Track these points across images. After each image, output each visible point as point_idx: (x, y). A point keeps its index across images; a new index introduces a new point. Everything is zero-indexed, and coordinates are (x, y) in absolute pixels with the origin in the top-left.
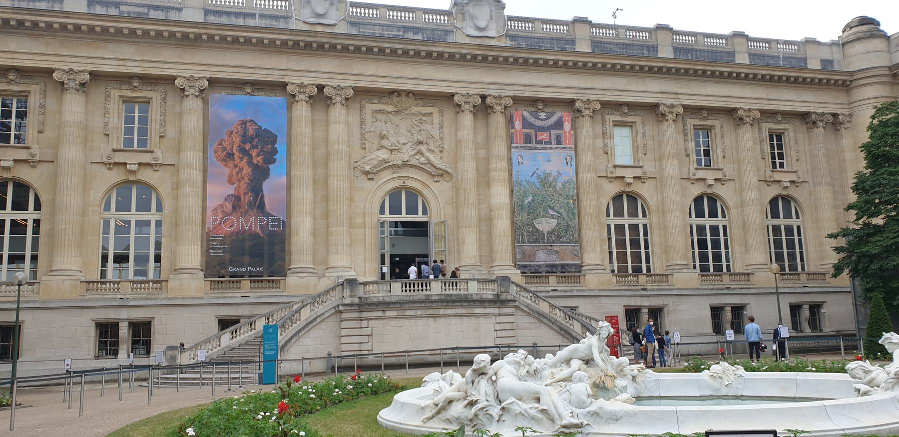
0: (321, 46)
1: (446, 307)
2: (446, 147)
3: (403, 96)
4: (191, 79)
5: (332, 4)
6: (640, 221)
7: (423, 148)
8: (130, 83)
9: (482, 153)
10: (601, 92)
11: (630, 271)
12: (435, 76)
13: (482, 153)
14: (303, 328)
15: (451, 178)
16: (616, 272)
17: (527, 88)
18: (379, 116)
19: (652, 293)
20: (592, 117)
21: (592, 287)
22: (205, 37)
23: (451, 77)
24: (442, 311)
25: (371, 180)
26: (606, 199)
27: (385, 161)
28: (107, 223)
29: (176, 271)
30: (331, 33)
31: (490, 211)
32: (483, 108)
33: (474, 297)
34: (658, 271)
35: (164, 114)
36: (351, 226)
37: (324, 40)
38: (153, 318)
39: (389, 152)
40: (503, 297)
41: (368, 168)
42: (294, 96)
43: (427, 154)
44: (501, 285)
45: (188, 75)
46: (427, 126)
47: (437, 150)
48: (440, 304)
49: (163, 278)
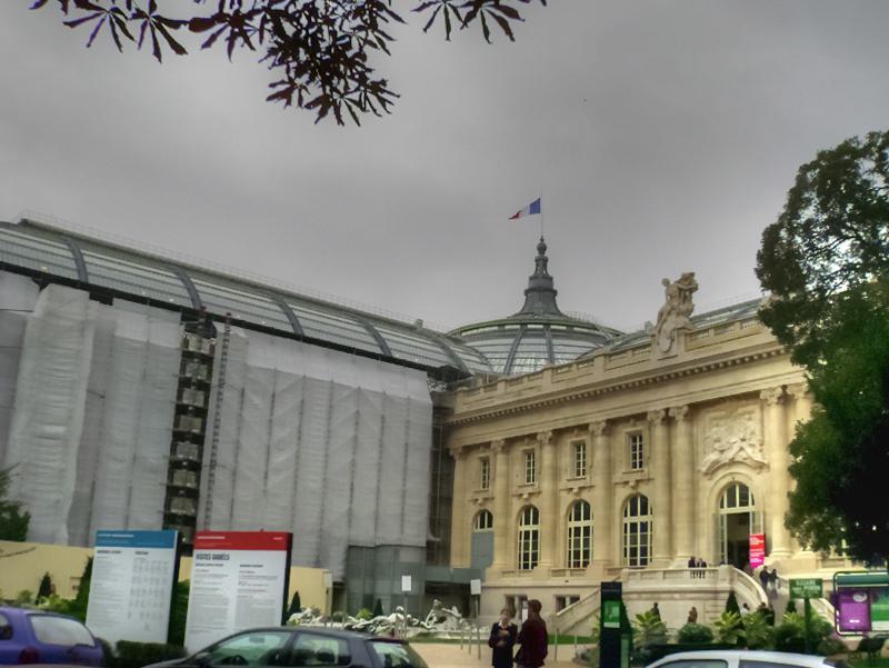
7: (744, 444)
27: (716, 462)
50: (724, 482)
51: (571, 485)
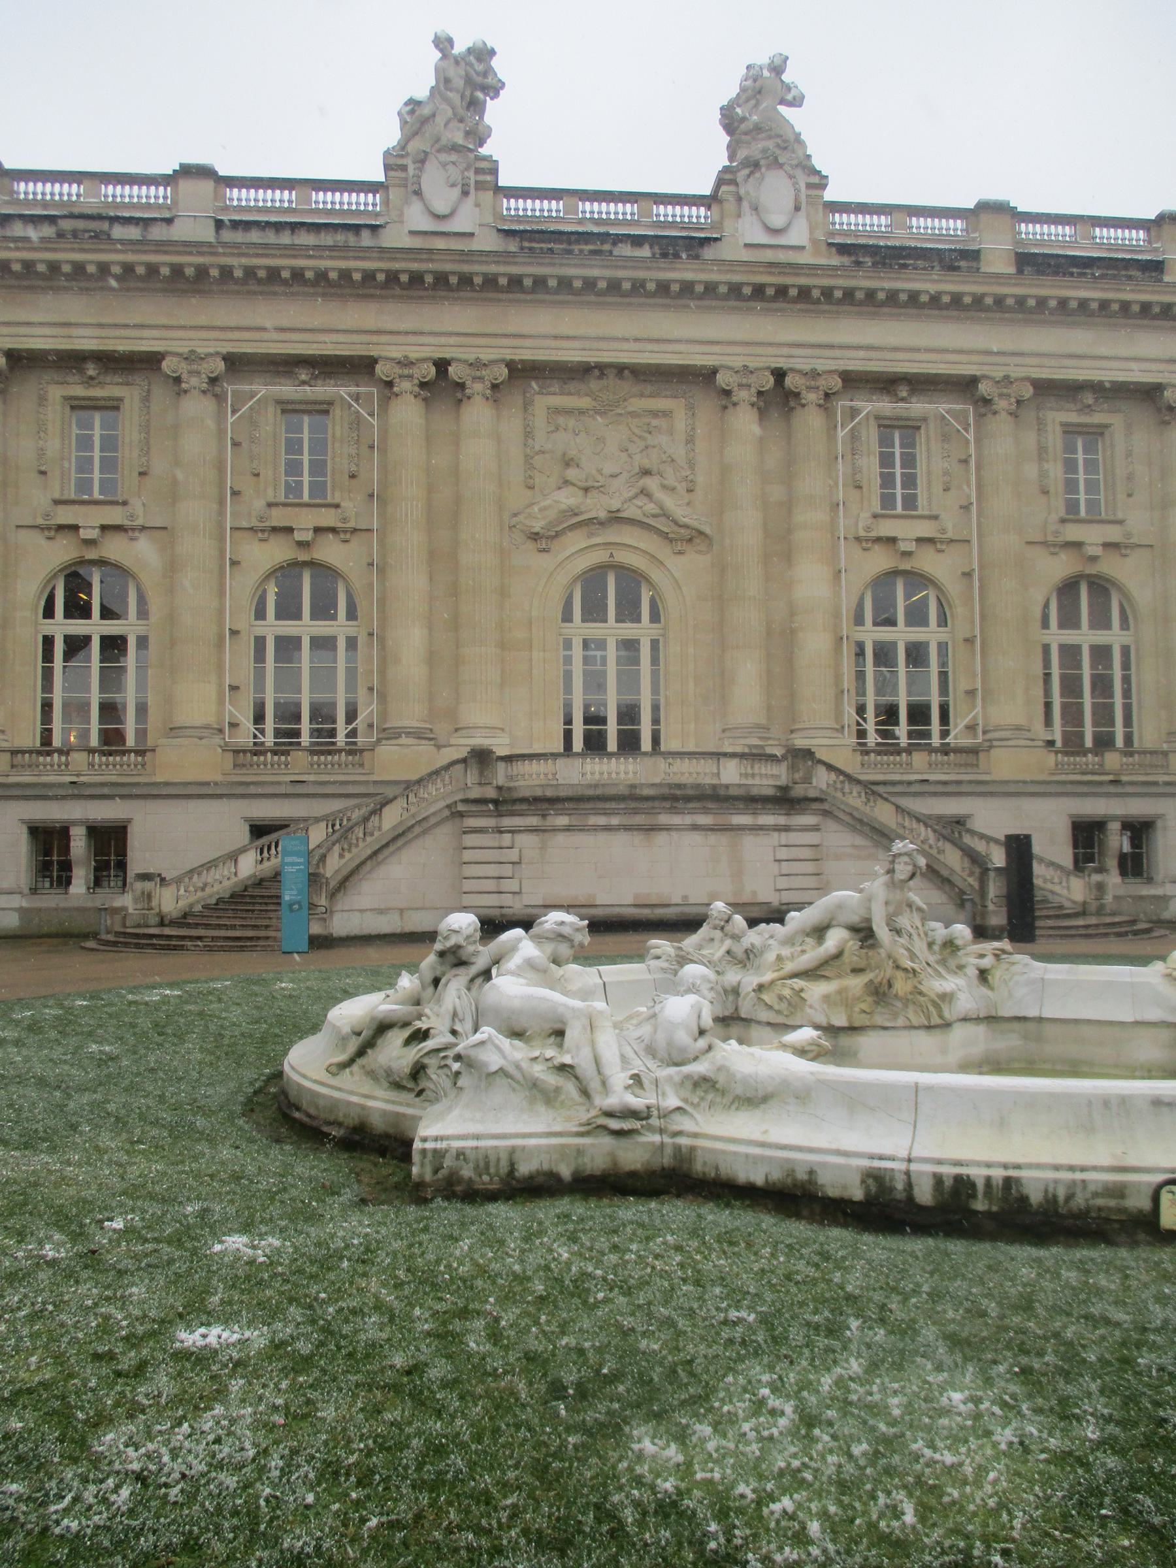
0: (441, 280)
1: (674, 810)
2: (700, 479)
3: (611, 376)
4: (191, 357)
5: (465, 193)
6: (1115, 637)
7: (651, 483)
8: (82, 371)
9: (777, 492)
11: (1089, 743)
12: (676, 334)
13: (777, 492)
14: (387, 845)
15: (711, 545)
16: (1059, 744)
17: (873, 354)
18: (561, 420)
19: (1130, 789)
20: (1014, 415)
21: (1006, 776)
22: (214, 272)
24: (664, 819)
25: (544, 551)
26: (1040, 593)
28: (48, 641)
29: (174, 731)
30: (462, 253)
31: (792, 614)
32: (779, 395)
33: (733, 792)
34: (1149, 745)
35: (146, 428)
36: (502, 645)
37: (448, 267)
38: (129, 821)
39: (581, 493)
40: (798, 791)
41: (537, 526)
42: (390, 384)
43: (659, 495)
44: (793, 768)
45: (186, 350)
46: (663, 440)
47: (681, 488)
48: (657, 804)
49: (150, 743)
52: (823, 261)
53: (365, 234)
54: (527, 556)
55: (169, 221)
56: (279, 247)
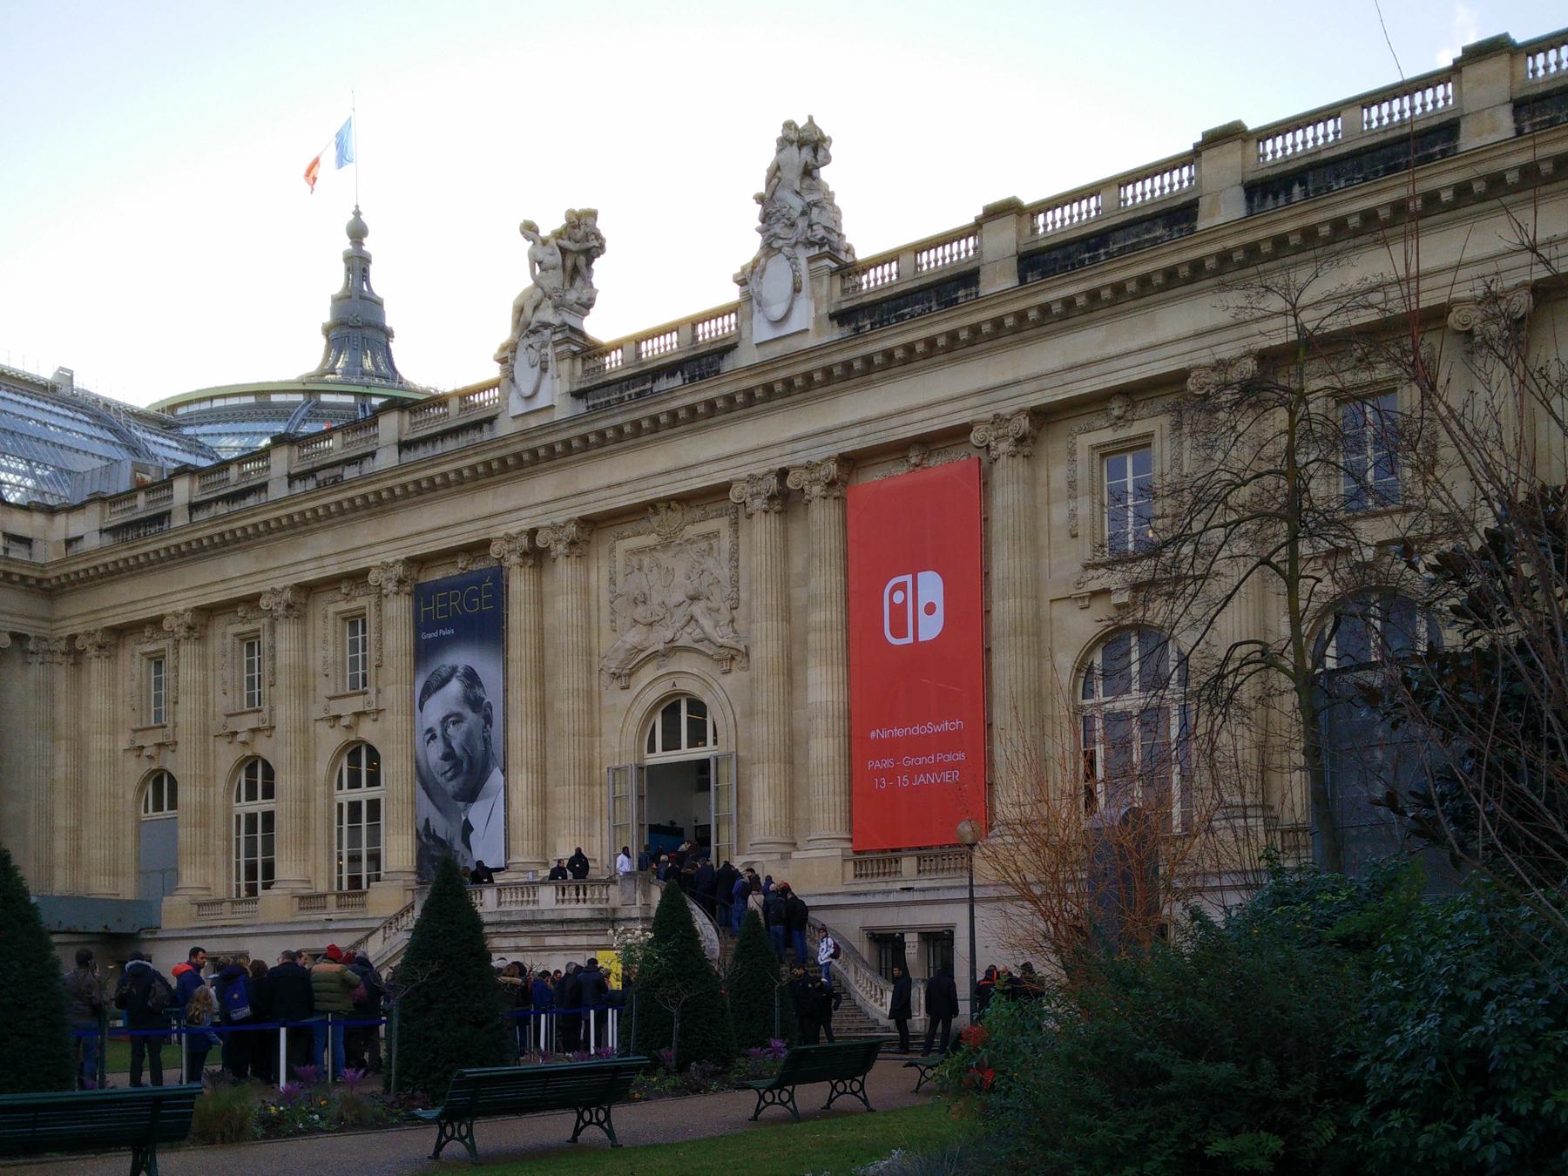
5: (544, 370)
7: (698, 609)
10: (1033, 386)
23: (728, 448)
32: (785, 498)
39: (645, 629)
46: (710, 563)
50: (653, 696)
51: (336, 708)
52: (826, 340)
53: (486, 427)
54: (616, 699)
55: (373, 454)
56: (444, 455)
